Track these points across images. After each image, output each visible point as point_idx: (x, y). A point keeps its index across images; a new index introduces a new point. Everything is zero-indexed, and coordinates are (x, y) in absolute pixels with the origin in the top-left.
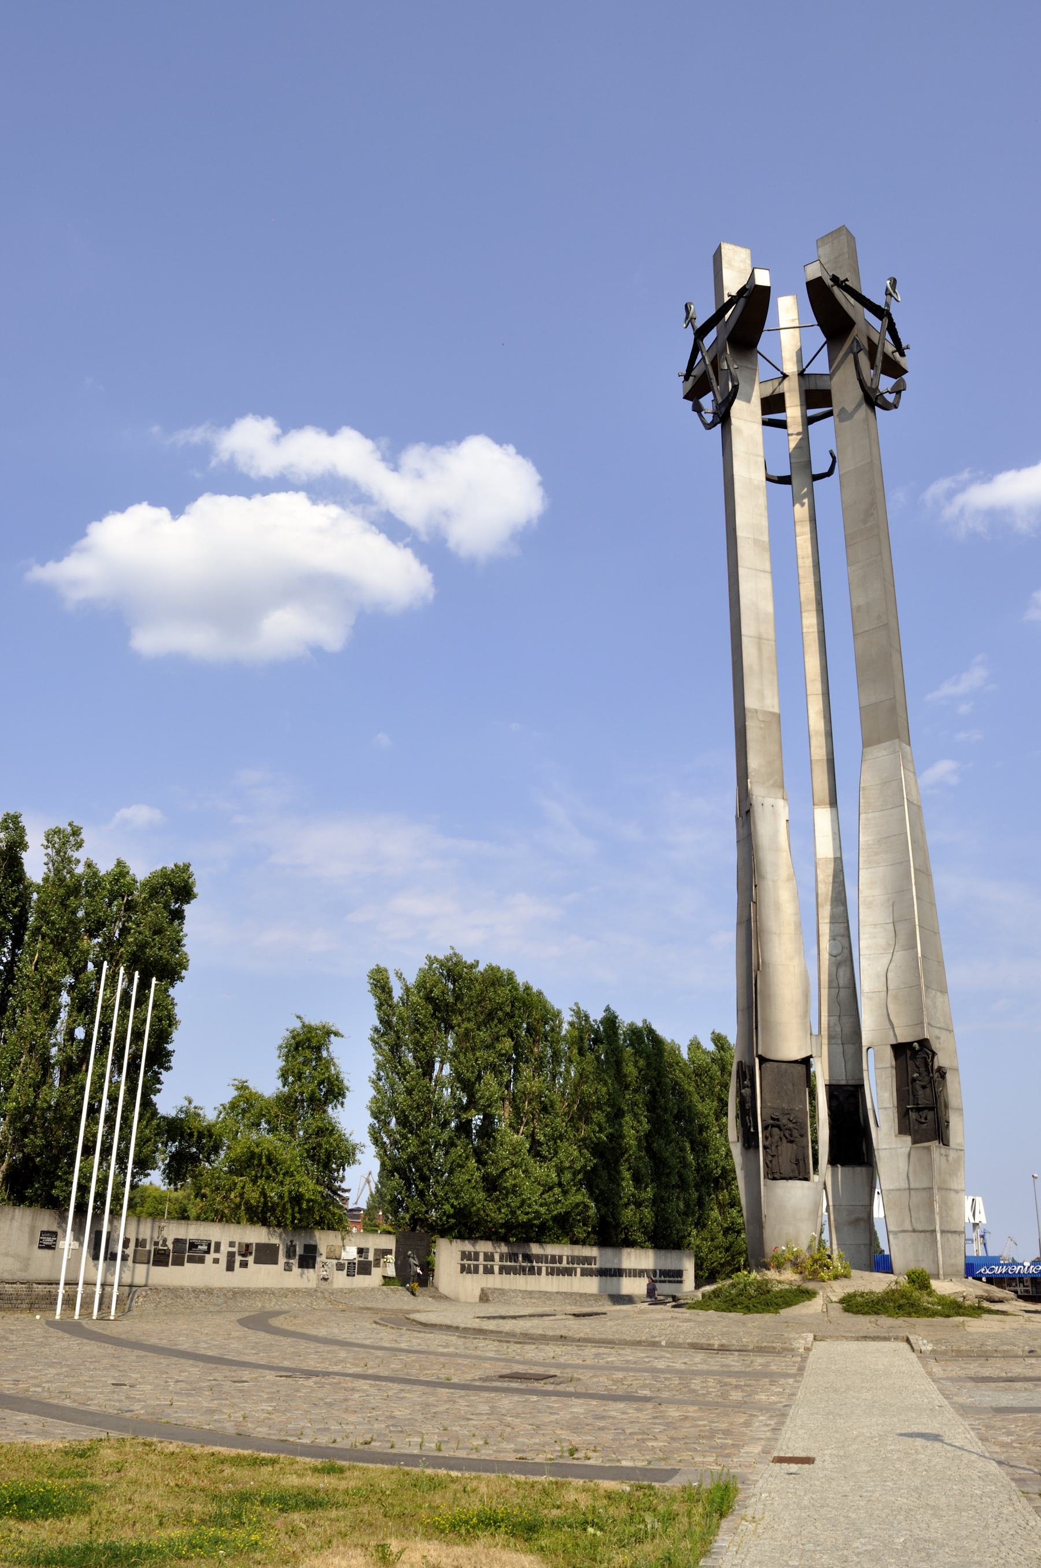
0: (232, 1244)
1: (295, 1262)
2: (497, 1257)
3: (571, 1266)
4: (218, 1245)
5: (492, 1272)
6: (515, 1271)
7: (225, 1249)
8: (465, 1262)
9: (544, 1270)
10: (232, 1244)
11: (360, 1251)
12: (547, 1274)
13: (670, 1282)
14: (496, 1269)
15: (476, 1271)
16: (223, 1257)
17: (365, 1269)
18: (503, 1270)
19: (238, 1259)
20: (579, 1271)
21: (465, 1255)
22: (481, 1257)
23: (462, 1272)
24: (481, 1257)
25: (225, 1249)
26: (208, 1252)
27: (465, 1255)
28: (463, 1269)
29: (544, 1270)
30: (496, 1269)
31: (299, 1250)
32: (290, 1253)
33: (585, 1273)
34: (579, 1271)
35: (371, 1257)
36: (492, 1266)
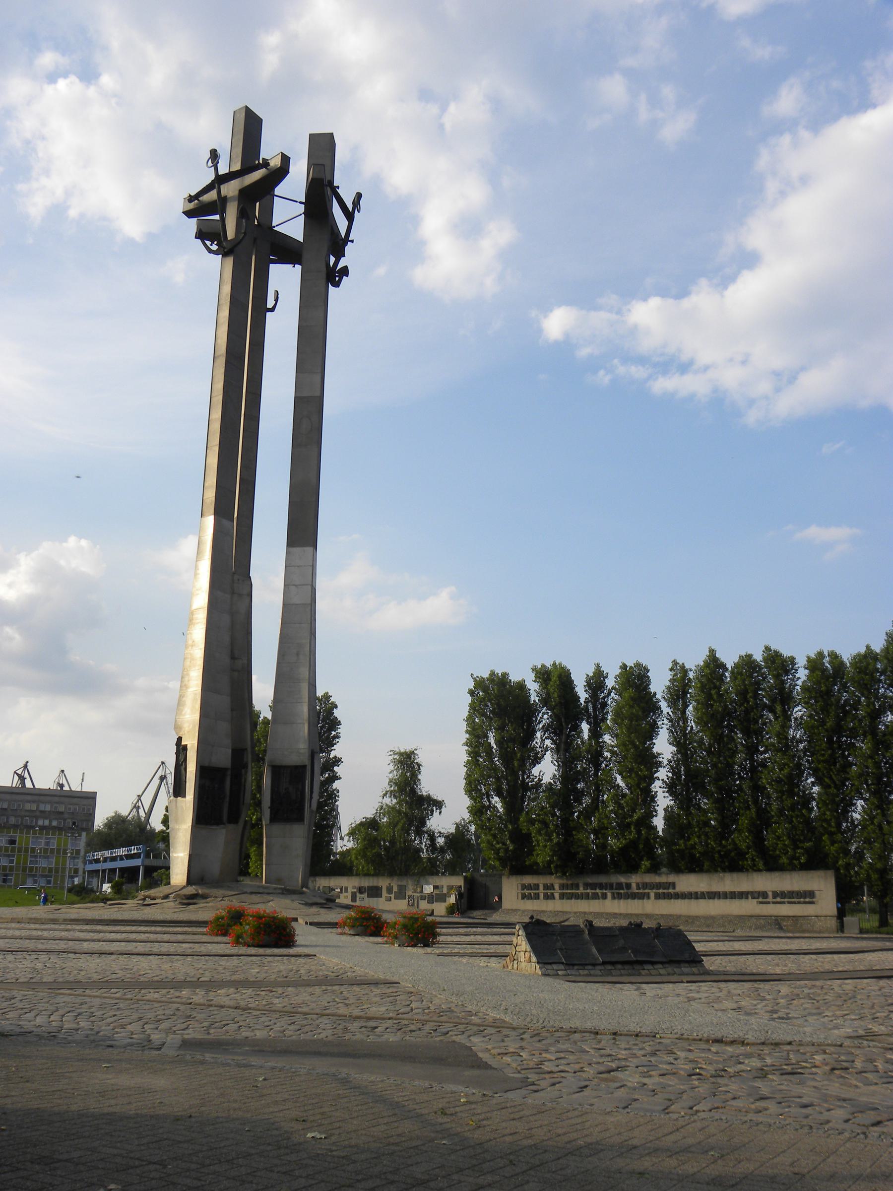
0: (354, 887)
1: (393, 896)
2: (557, 887)
3: (641, 891)
4: (346, 889)
5: (554, 899)
6: (570, 897)
7: (350, 890)
8: (527, 892)
9: (609, 895)
10: (354, 887)
11: (436, 887)
12: (614, 898)
13: (789, 903)
14: (557, 895)
15: (537, 897)
16: (349, 895)
17: (442, 898)
18: (562, 896)
19: (358, 895)
20: (652, 895)
21: (524, 887)
22: (541, 887)
23: (523, 898)
24: (541, 887)
25: (350, 890)
26: (341, 892)
27: (524, 887)
28: (524, 897)
29: (609, 895)
30: (557, 895)
31: (395, 889)
32: (390, 890)
33: (658, 897)
34: (652, 895)
35: (445, 891)
36: (552, 894)
